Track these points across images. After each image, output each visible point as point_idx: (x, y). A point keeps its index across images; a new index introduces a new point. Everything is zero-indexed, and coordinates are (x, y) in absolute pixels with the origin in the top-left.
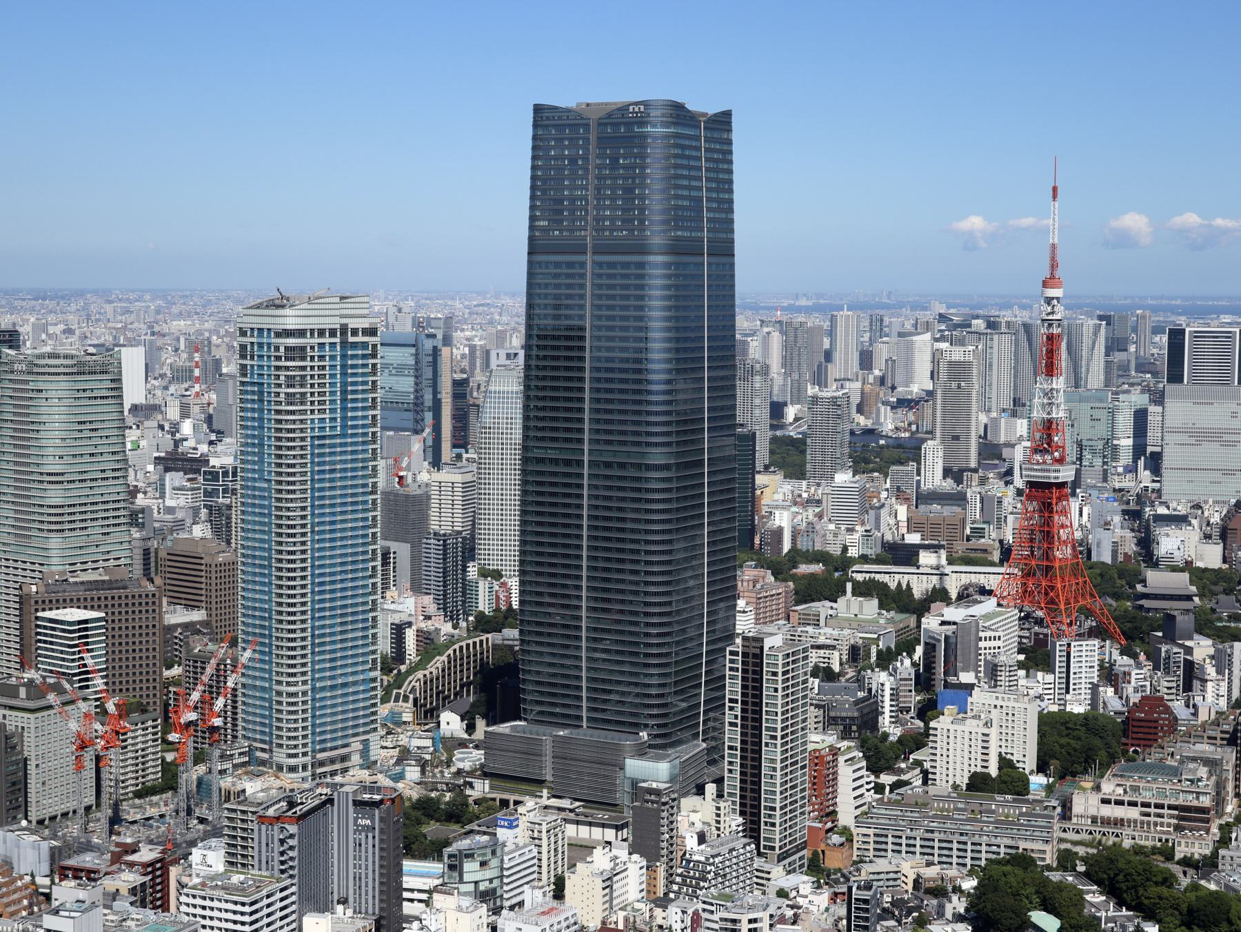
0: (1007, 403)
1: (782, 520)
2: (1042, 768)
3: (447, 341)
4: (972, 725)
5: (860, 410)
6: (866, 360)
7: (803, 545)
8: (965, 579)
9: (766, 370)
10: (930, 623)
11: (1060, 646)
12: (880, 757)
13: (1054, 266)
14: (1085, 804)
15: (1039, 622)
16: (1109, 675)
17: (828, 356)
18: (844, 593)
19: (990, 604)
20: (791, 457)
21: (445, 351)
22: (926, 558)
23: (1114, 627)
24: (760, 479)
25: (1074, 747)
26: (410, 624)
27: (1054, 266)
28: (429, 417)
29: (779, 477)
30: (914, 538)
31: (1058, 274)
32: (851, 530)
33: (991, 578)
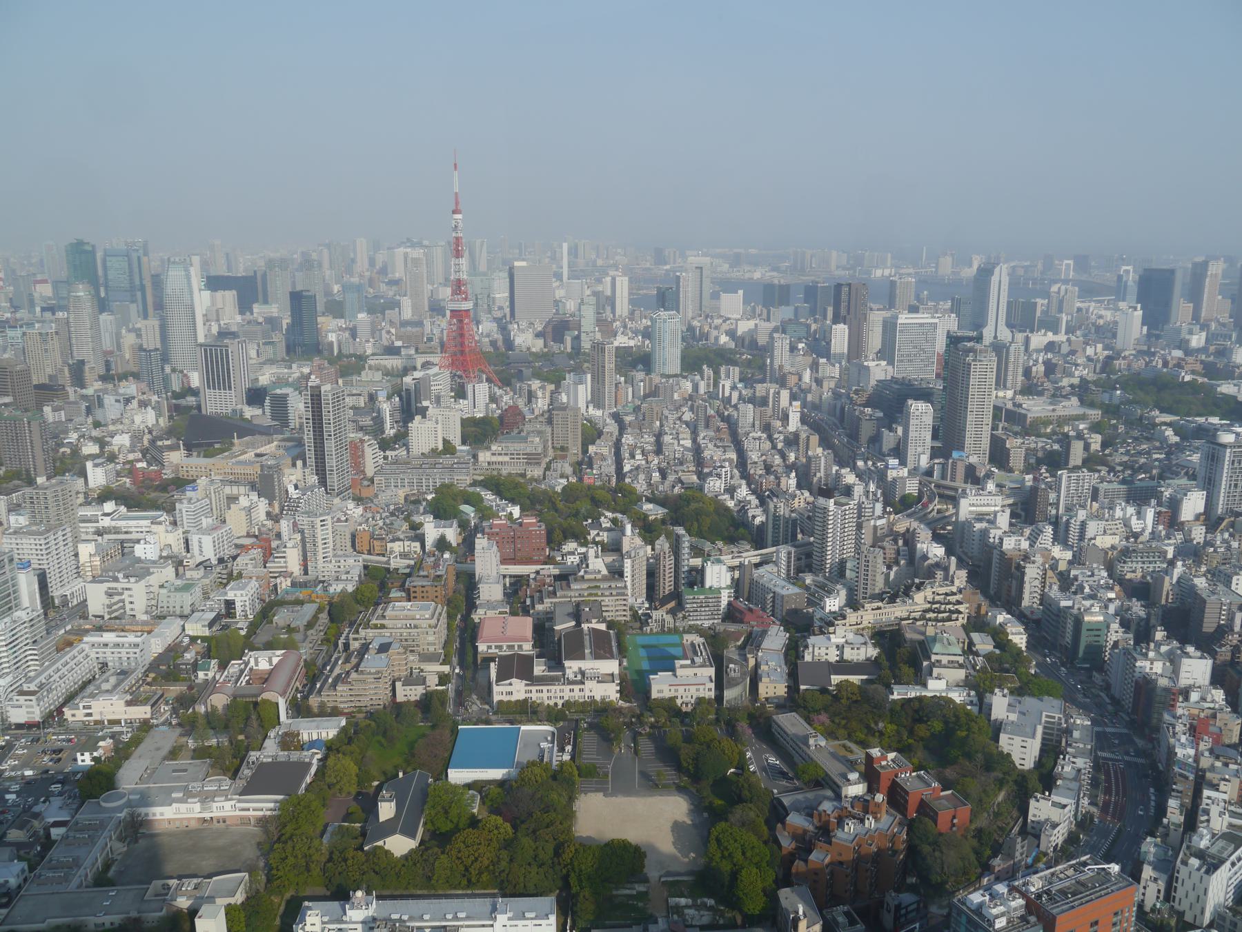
0: (442, 280)
1: (332, 337)
2: (464, 443)
3: (146, 254)
4: (429, 424)
5: (370, 286)
6: (372, 262)
7: (344, 352)
8: (424, 360)
9: (320, 265)
10: (408, 380)
11: (469, 388)
12: (385, 445)
13: (457, 203)
14: (484, 456)
15: (460, 377)
16: (493, 399)
17: (353, 261)
18: (364, 368)
19: (436, 370)
20: (336, 309)
21: (144, 259)
22: (403, 352)
23: (494, 377)
24: (319, 319)
25: (478, 432)
26: (134, 398)
27: (457, 203)
28: (139, 294)
29: (330, 318)
30: (399, 343)
31: (460, 207)
32: (368, 341)
33: (435, 359)
